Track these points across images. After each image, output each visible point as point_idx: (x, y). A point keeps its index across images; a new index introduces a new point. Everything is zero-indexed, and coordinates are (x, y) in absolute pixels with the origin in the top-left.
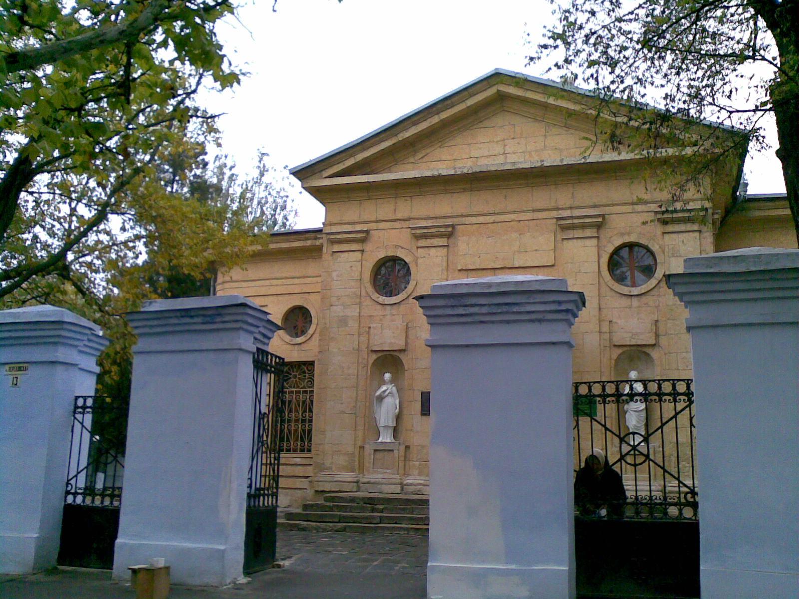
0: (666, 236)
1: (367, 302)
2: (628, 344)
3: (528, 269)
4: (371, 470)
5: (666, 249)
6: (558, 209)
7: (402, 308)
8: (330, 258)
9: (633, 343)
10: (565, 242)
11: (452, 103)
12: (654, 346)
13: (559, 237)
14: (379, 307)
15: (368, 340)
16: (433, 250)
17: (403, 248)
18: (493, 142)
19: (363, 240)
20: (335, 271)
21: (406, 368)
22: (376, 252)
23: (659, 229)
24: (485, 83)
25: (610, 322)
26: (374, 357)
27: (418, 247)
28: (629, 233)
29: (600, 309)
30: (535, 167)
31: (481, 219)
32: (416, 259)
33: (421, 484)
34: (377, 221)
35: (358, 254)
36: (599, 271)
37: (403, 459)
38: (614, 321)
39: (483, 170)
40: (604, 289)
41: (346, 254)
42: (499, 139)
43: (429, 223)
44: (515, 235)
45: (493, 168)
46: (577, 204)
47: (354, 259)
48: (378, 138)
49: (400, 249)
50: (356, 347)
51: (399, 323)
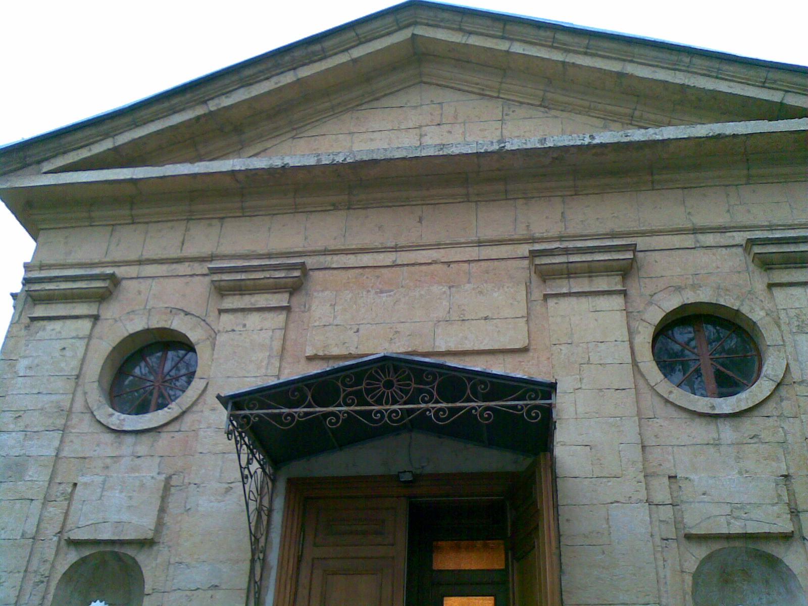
0: (778, 293)
1: (85, 425)
2: (725, 531)
5: (782, 315)
6: (534, 240)
7: (164, 441)
9: (737, 528)
10: (551, 303)
11: (323, 50)
12: (786, 537)
13: (537, 294)
14: (108, 437)
15: (66, 514)
16: (254, 320)
17: (187, 314)
18: (399, 130)
19: (103, 297)
20: (25, 357)
21: (148, 588)
22: (125, 320)
23: (759, 281)
24: (389, 20)
26: (73, 556)
27: (221, 311)
29: (644, 447)
31: (366, 259)
32: (213, 335)
34: (140, 262)
35: (86, 325)
36: (635, 363)
39: (375, 157)
40: (649, 400)
41: (58, 325)
42: (411, 125)
45: (398, 155)
46: (571, 231)
47: (74, 334)
48: (166, 105)
49: (183, 314)
50: (31, 529)
51: (150, 473)
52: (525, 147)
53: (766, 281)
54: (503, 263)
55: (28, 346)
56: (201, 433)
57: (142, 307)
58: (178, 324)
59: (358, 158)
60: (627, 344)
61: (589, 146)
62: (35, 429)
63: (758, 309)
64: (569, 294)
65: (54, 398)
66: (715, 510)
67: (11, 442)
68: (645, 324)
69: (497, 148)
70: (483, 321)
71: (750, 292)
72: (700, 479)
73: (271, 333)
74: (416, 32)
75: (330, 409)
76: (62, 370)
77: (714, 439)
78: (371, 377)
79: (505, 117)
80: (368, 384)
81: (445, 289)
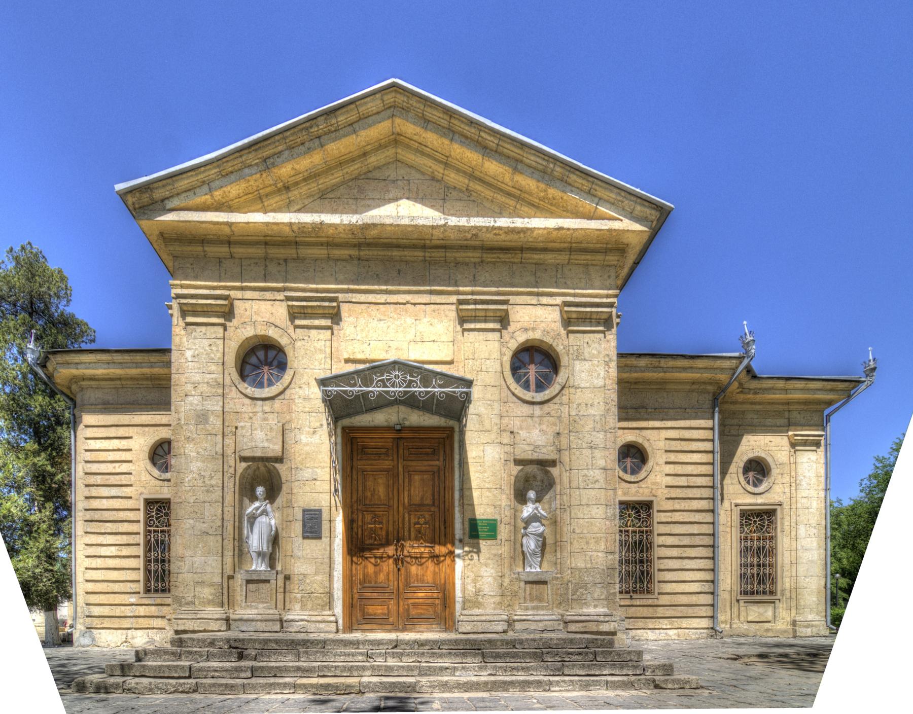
1: (233, 393)
4: (243, 604)
5: (571, 351)
7: (277, 403)
8: (183, 332)
14: (247, 401)
16: (314, 332)
17: (276, 326)
22: (242, 331)
25: (512, 432)
28: (534, 329)
33: (303, 620)
35: (220, 330)
37: (282, 590)
38: (515, 431)
41: (203, 329)
44: (410, 320)
47: (214, 336)
56: (297, 401)
66: (527, 448)
67: (196, 402)
72: (523, 434)
76: (213, 359)
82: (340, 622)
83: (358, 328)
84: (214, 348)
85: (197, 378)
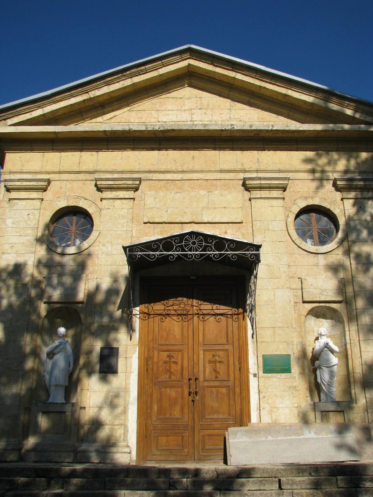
3: (217, 225)
8: (7, 205)
30: (225, 130)
31: (169, 176)
34: (60, 172)
35: (38, 203)
39: (174, 128)
41: (24, 202)
42: (186, 108)
43: (116, 176)
44: (202, 192)
45: (184, 128)
47: (33, 208)
49: (83, 200)
52: (243, 128)
53: (341, 196)
54: (231, 181)
55: (10, 212)
56: (100, 256)
57: (63, 195)
58: (82, 204)
59: (166, 128)
60: (284, 222)
61: (272, 130)
62: (21, 252)
63: (337, 209)
64: (261, 198)
65: (28, 238)
68: (292, 213)
69: (231, 128)
70: (223, 209)
71: (334, 201)
73: (127, 211)
74: (190, 63)
75: (170, 253)
76: (29, 225)
77: (316, 263)
78: (186, 240)
79: (232, 108)
80: (185, 243)
81: (206, 193)
82: (134, 453)
83: (157, 200)
84: (31, 217)
85: (15, 240)
